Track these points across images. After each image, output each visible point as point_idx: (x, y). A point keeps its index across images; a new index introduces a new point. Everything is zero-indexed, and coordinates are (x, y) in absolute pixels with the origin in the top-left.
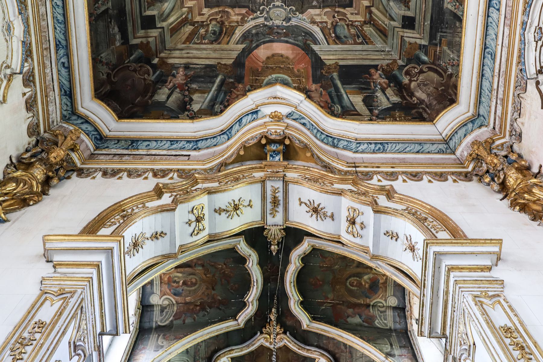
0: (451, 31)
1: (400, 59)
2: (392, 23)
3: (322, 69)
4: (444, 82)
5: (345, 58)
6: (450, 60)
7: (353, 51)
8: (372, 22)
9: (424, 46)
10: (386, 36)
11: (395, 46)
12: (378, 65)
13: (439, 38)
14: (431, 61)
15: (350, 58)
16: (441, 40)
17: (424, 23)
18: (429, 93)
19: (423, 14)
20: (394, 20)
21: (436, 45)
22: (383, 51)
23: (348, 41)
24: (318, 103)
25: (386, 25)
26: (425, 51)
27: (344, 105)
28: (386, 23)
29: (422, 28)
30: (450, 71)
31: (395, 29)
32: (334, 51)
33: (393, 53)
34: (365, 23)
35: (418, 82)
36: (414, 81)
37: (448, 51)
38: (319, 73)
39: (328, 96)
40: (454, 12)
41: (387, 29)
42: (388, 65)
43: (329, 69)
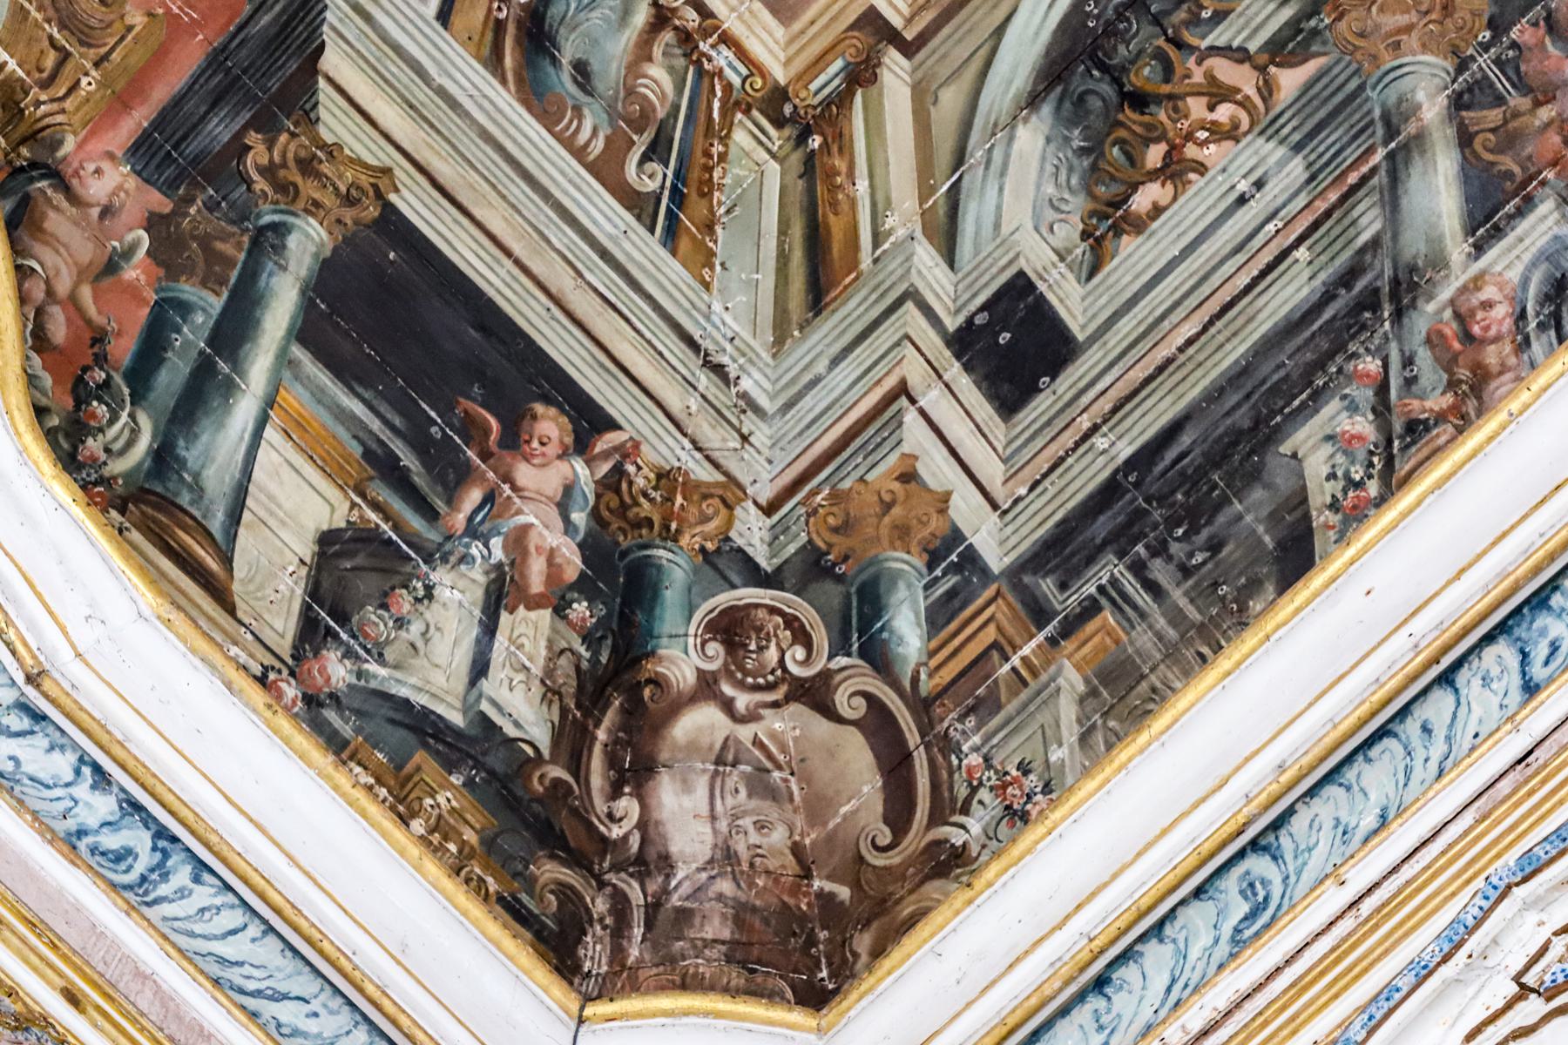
0: (1194, 614)
1: (769, 510)
2: (926, 256)
3: (266, 124)
4: (879, 861)
5: (462, 198)
6: (1024, 769)
7: (546, 195)
8: (816, 142)
9: (971, 559)
10: (818, 297)
11: (813, 403)
12: (614, 426)
13: (1091, 589)
14: (927, 686)
15: (496, 227)
16: (1090, 609)
17: (1095, 429)
18: (741, 847)
19: (1139, 374)
20: (950, 255)
21: (1039, 613)
22: (718, 370)
23: (577, 109)
24: (39, 294)
25: (877, 240)
26: (951, 594)
27: (191, 455)
28: (889, 223)
29: (1056, 449)
30: (971, 829)
31: (909, 305)
32: (442, 92)
33: (761, 435)
34: (775, 103)
35: (745, 733)
36: (728, 706)
37: (1067, 710)
38: (219, 130)
39: (145, 312)
40: (1307, 517)
41: (866, 262)
42: (666, 478)
43: (307, 166)
